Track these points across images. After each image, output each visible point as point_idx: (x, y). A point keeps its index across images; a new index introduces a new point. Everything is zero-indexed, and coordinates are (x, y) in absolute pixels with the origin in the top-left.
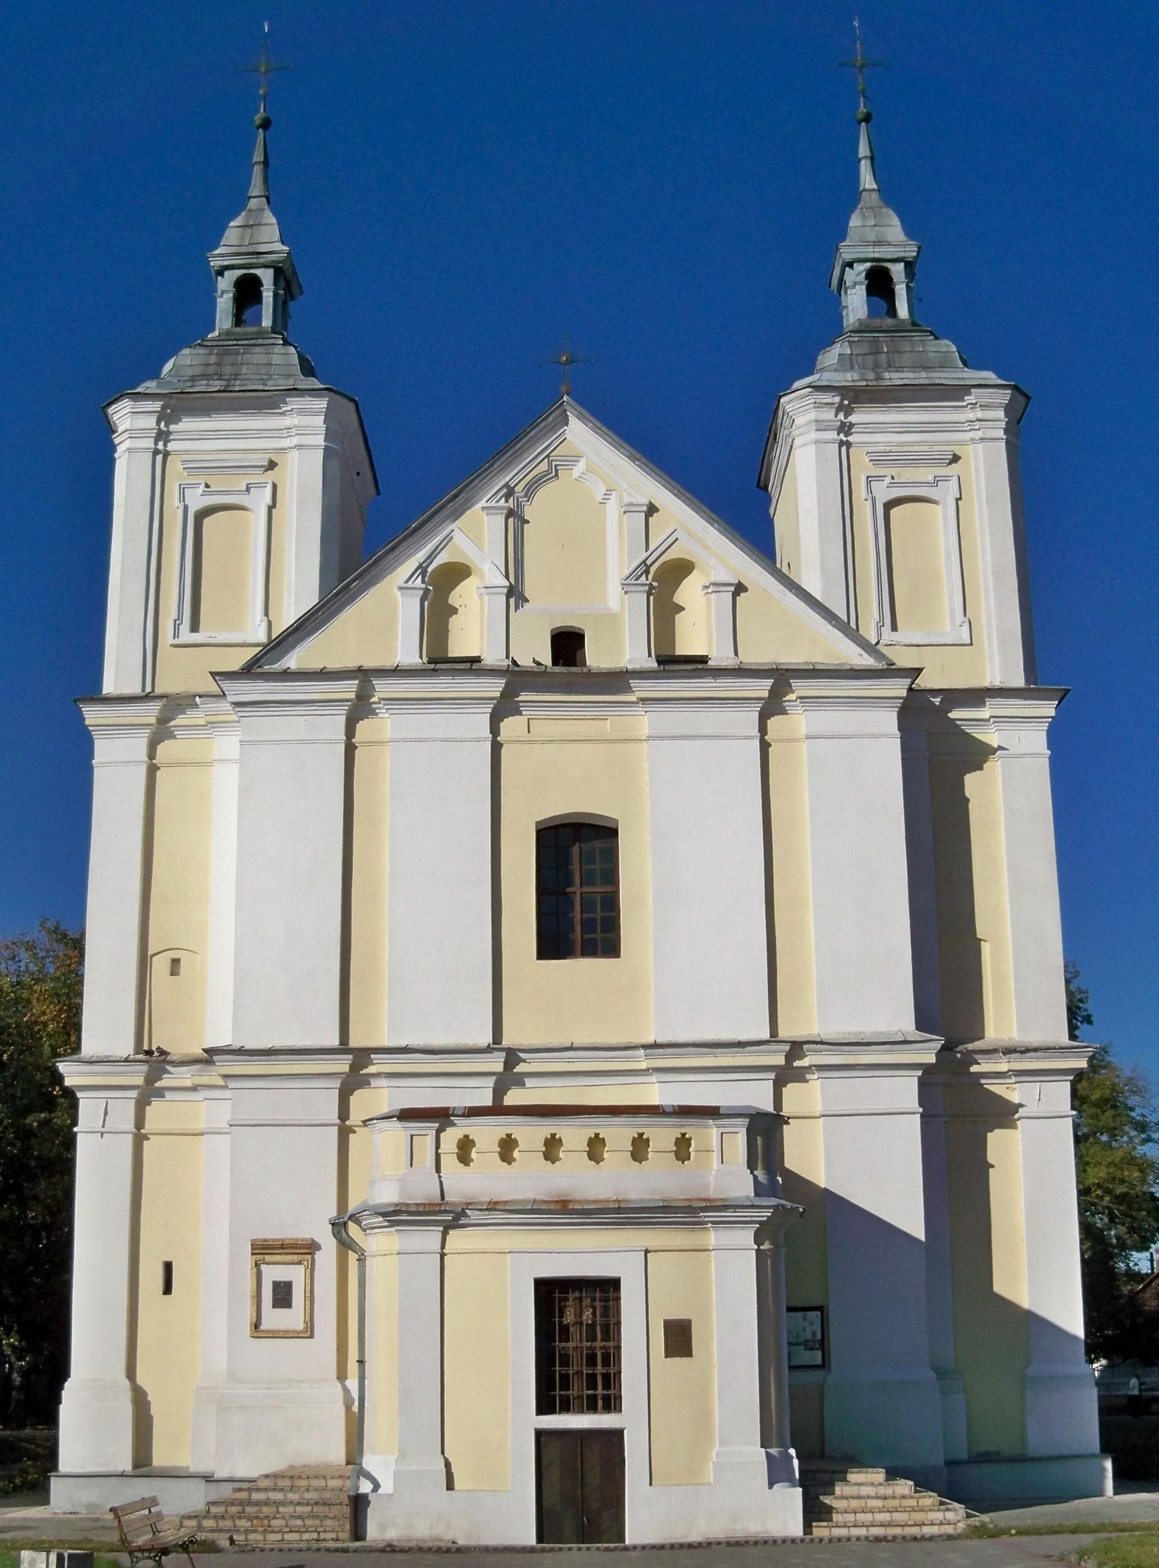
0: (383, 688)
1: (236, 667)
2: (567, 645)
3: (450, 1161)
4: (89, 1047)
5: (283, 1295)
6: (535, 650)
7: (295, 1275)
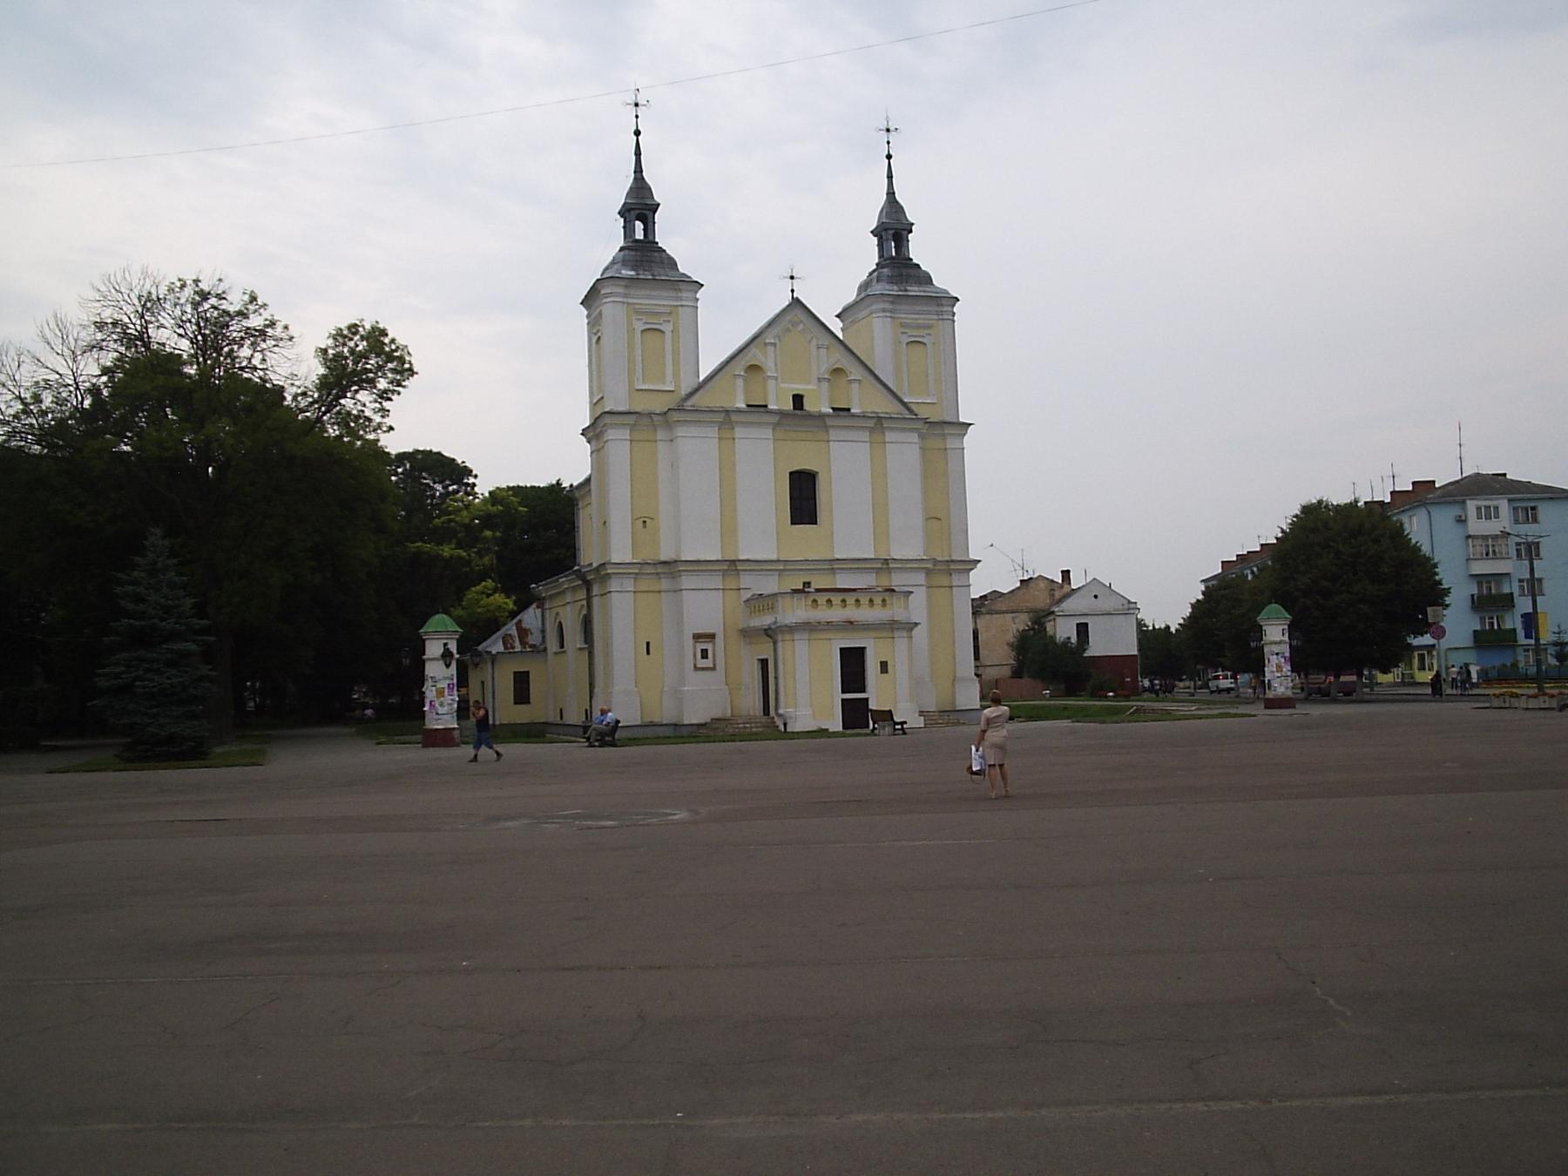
0: (734, 418)
2: (798, 400)
5: (704, 654)
7: (709, 647)
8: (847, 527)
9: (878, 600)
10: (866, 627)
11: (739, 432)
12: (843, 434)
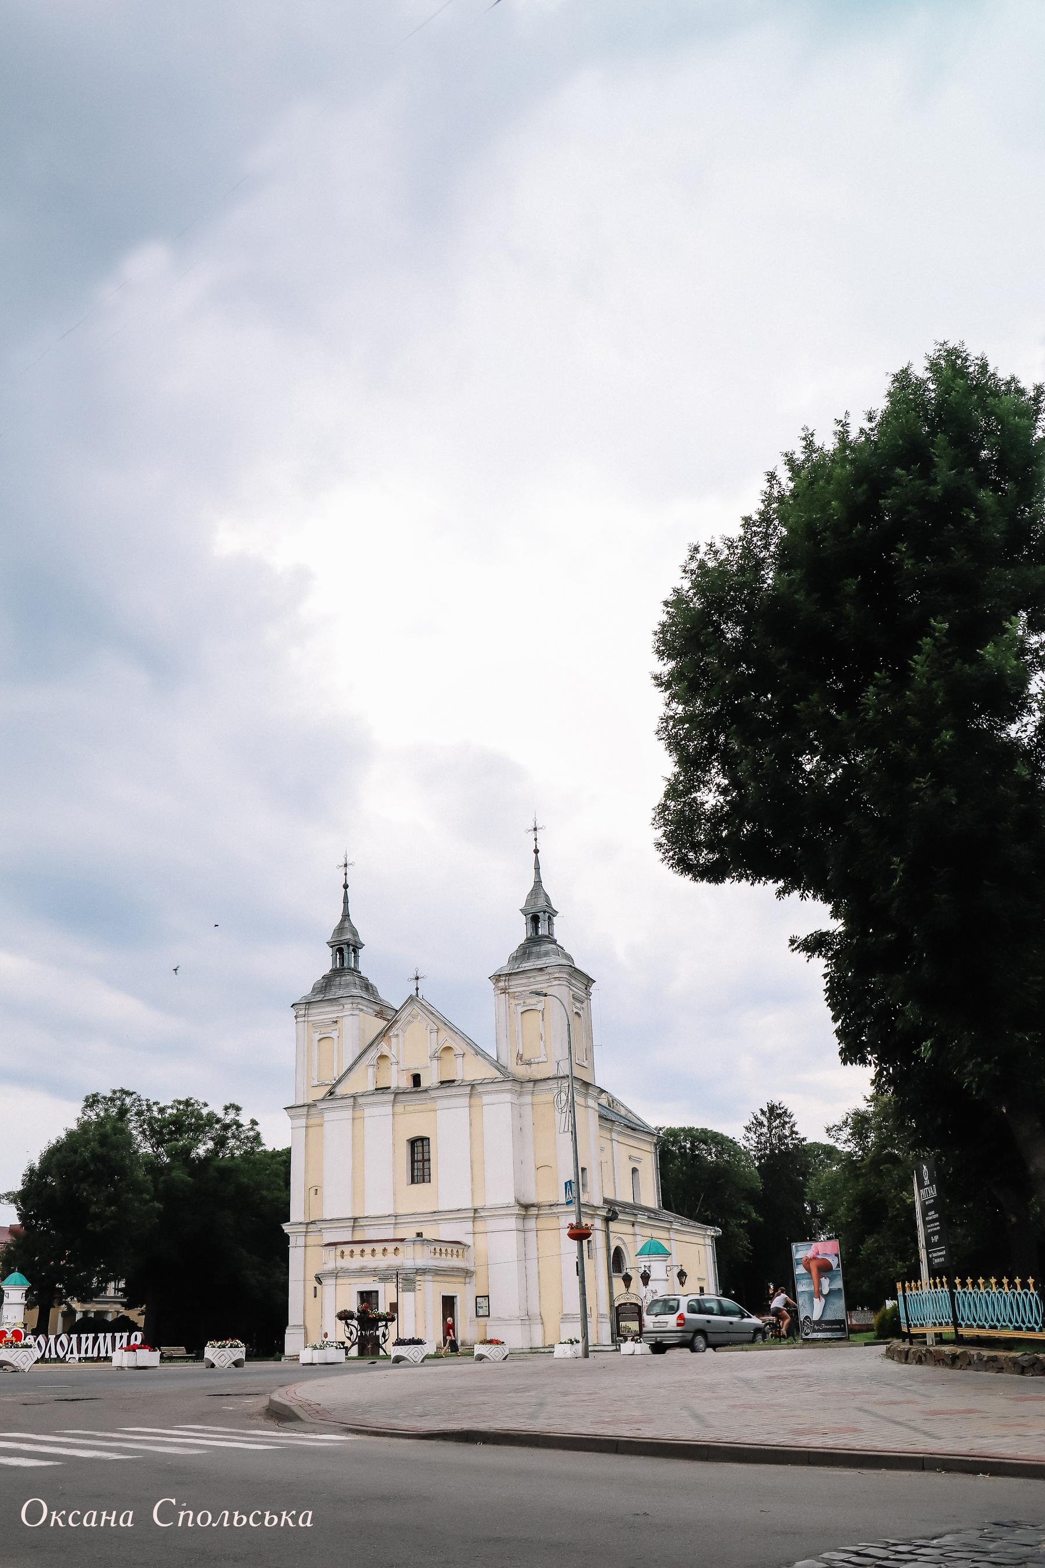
1: (321, 1097)
2: (416, 1079)
3: (339, 1258)
4: (293, 1219)
6: (406, 1083)
8: (450, 1184)
9: (347, 1252)
10: (374, 1272)
11: (368, 1111)
12: (444, 1103)
